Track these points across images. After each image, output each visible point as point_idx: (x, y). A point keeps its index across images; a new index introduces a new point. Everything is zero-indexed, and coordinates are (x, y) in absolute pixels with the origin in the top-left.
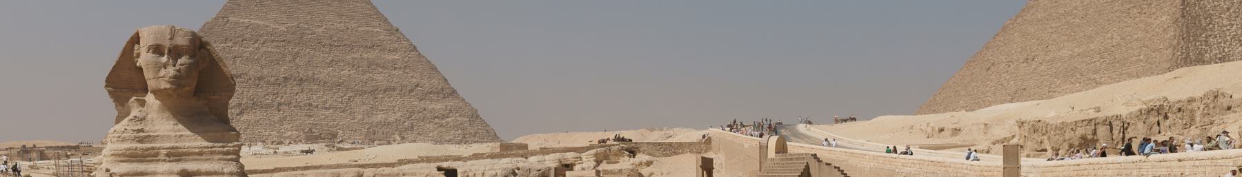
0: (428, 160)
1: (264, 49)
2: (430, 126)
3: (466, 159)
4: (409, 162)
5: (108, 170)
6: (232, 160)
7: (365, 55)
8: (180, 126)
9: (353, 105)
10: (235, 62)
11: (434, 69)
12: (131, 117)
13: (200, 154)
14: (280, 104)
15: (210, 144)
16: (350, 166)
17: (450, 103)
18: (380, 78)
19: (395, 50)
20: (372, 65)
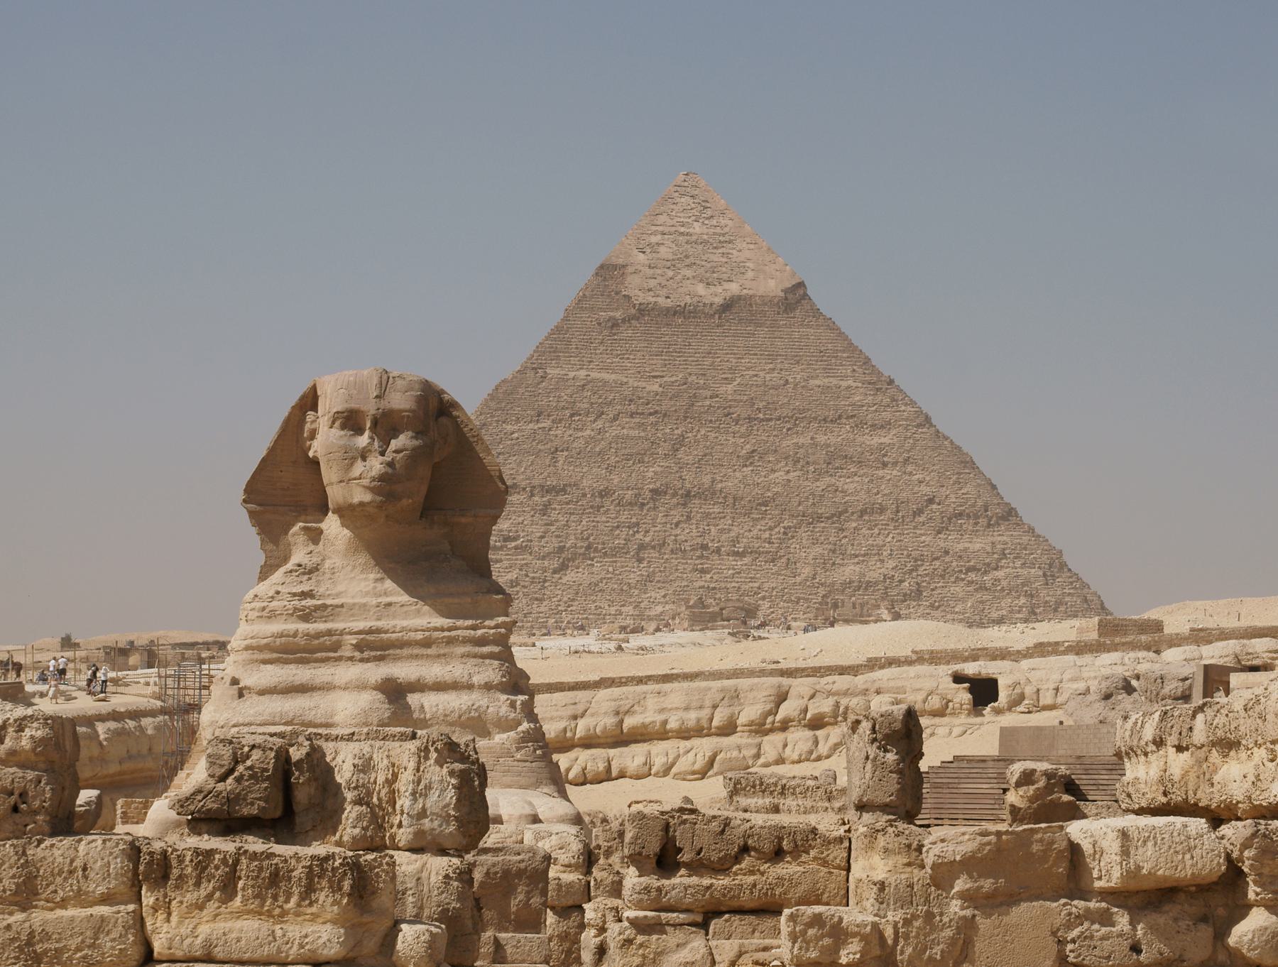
0: (934, 658)
1: (613, 431)
2: (958, 589)
3: (1017, 656)
4: (891, 662)
5: (235, 682)
6: (491, 656)
7: (821, 439)
8: (389, 584)
9: (794, 545)
10: (555, 460)
11: (969, 464)
12: (289, 566)
13: (427, 643)
14: (642, 547)
15: (446, 622)
16: (762, 673)
17: (1003, 537)
18: (853, 486)
19: (885, 426)
20: (837, 459)
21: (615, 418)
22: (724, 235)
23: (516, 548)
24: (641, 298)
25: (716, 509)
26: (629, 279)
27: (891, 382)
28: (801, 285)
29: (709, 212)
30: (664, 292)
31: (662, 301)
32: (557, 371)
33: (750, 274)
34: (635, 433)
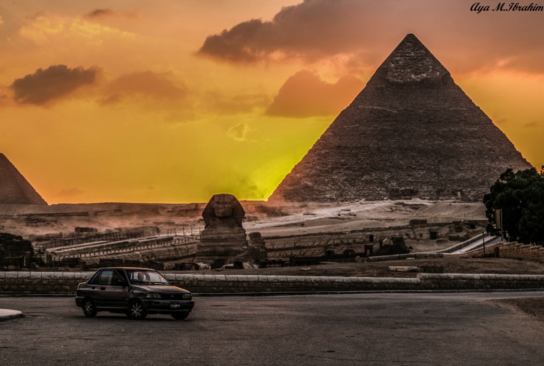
11: (504, 136)
19: (477, 124)
21: (382, 122)
22: (422, 56)
23: (347, 168)
24: (391, 79)
25: (416, 154)
26: (388, 73)
27: (478, 108)
28: (448, 73)
29: (417, 48)
30: (400, 77)
31: (398, 80)
32: (363, 106)
33: (431, 70)
34: (388, 128)
